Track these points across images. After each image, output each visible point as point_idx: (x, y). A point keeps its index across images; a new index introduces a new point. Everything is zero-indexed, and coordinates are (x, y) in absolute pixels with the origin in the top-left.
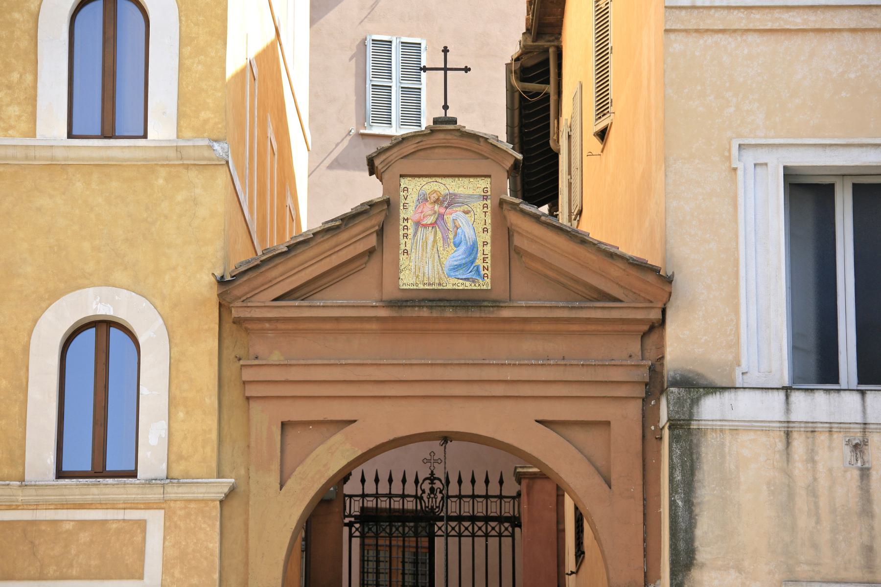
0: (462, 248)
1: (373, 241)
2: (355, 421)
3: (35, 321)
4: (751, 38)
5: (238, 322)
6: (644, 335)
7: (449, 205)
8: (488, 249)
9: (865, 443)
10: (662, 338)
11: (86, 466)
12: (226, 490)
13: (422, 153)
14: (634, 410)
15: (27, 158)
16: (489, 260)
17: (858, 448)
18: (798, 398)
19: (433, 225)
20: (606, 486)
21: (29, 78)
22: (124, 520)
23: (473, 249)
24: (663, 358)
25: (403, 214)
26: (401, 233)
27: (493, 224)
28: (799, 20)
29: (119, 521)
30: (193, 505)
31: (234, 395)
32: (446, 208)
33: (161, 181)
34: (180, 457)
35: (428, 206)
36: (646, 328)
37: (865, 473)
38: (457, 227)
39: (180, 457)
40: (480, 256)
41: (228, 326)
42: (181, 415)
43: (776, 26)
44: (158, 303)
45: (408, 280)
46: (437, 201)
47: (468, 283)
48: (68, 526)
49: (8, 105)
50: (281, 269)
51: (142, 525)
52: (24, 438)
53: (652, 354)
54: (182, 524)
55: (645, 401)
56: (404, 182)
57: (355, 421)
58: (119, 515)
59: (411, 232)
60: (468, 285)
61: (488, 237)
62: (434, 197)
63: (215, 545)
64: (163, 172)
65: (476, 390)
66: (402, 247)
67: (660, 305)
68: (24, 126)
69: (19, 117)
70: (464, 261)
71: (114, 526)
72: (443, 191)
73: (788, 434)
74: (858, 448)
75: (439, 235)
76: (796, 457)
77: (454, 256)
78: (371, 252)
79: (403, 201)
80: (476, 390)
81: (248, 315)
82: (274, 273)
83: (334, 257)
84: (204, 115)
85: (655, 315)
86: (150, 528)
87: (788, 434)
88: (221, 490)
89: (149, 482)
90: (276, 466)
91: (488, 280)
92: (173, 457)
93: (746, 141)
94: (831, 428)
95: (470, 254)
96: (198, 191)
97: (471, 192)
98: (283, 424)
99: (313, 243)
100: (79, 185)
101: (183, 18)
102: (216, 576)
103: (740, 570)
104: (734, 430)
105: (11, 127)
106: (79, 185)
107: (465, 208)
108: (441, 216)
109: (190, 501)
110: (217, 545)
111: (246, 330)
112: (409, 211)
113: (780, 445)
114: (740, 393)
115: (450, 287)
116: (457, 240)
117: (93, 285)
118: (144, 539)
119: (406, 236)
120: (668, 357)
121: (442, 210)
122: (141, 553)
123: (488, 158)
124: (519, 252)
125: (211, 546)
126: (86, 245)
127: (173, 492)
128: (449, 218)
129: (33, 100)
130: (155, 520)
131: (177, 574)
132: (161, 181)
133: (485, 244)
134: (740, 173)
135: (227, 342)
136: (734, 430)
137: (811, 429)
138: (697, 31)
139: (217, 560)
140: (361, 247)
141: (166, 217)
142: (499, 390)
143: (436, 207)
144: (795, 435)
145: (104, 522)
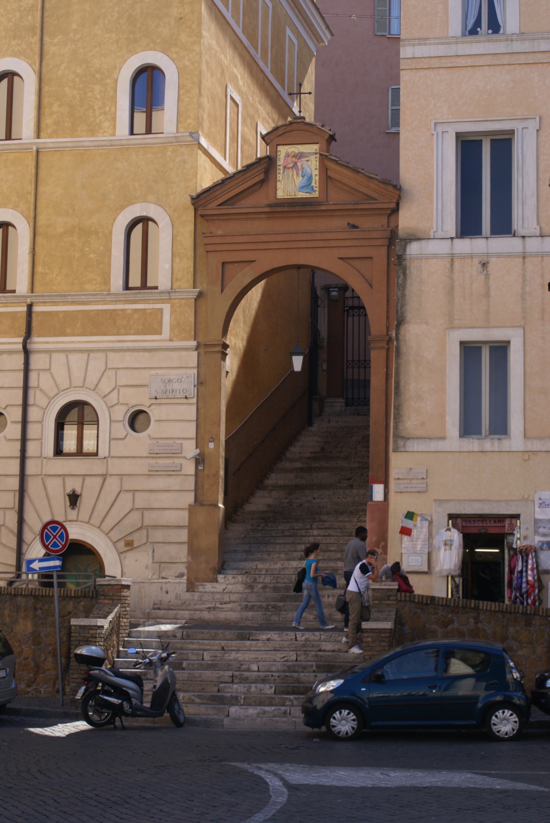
0: (306, 178)
1: (262, 177)
2: (255, 261)
3: (115, 220)
4: (442, 71)
5: (202, 216)
6: (389, 215)
7: (300, 158)
8: (317, 178)
9: (488, 262)
10: (398, 216)
11: (139, 285)
12: (197, 294)
13: (287, 134)
14: (384, 250)
15: (111, 146)
16: (318, 183)
17: (484, 265)
18: (457, 242)
19: (292, 168)
20: (369, 287)
21: (113, 109)
22: (153, 309)
23: (310, 178)
24: (398, 226)
25: (278, 163)
26: (278, 172)
27: (319, 166)
28: (463, 62)
29: (151, 309)
30: (183, 301)
31: (201, 250)
32: (298, 159)
33: (169, 153)
34: (177, 280)
35: (290, 158)
36: (389, 212)
37: (487, 276)
38: (303, 168)
39: (177, 280)
40: (314, 181)
41: (199, 218)
42: (177, 260)
43: (452, 65)
44: (167, 209)
45: (280, 194)
46: (294, 156)
47: (308, 194)
48: (129, 312)
49: (104, 122)
50: (220, 191)
51: (161, 311)
52: (110, 273)
53: (392, 225)
55: (389, 246)
56: (280, 148)
57: (255, 261)
59: (282, 171)
60: (308, 195)
61: (317, 172)
62: (293, 154)
63: (192, 319)
64: (170, 149)
65: (310, 244)
66: (278, 179)
67: (395, 201)
68: (110, 131)
69: (109, 127)
70: (306, 184)
71: (149, 311)
72: (297, 151)
73: (452, 260)
74: (484, 265)
75: (295, 172)
76: (455, 270)
77: (299, 181)
78: (262, 182)
79: (278, 157)
80: (310, 244)
81: (206, 213)
82: (217, 193)
83: (244, 184)
84: (189, 121)
85: (393, 205)
86: (164, 311)
87: (452, 260)
88: (194, 294)
89: (161, 292)
91: (317, 193)
92: (174, 280)
93: (438, 121)
94: (471, 256)
95: (309, 181)
97: (309, 151)
98: (223, 263)
99: (234, 179)
101: (180, 77)
102: (193, 333)
103: (427, 323)
104: (427, 258)
105: (105, 132)
107: (307, 159)
108: (296, 163)
110: (193, 319)
111: (207, 220)
112: (281, 161)
113: (448, 266)
114: (430, 241)
115: (299, 196)
116: (303, 174)
117: (139, 202)
119: (280, 173)
120: (400, 226)
121: (296, 161)
122: (161, 323)
123: (317, 135)
124: (331, 178)
125: (191, 319)
127: (173, 296)
128: (299, 164)
129: (114, 119)
130: (166, 308)
131: (176, 332)
132: (169, 153)
133: (316, 175)
134: (435, 136)
135: (199, 226)
136: (427, 258)
137: (463, 257)
138: (416, 69)
139: (193, 326)
140: (257, 179)
142: (321, 244)
143: (294, 159)
144: (456, 260)
145: (144, 310)
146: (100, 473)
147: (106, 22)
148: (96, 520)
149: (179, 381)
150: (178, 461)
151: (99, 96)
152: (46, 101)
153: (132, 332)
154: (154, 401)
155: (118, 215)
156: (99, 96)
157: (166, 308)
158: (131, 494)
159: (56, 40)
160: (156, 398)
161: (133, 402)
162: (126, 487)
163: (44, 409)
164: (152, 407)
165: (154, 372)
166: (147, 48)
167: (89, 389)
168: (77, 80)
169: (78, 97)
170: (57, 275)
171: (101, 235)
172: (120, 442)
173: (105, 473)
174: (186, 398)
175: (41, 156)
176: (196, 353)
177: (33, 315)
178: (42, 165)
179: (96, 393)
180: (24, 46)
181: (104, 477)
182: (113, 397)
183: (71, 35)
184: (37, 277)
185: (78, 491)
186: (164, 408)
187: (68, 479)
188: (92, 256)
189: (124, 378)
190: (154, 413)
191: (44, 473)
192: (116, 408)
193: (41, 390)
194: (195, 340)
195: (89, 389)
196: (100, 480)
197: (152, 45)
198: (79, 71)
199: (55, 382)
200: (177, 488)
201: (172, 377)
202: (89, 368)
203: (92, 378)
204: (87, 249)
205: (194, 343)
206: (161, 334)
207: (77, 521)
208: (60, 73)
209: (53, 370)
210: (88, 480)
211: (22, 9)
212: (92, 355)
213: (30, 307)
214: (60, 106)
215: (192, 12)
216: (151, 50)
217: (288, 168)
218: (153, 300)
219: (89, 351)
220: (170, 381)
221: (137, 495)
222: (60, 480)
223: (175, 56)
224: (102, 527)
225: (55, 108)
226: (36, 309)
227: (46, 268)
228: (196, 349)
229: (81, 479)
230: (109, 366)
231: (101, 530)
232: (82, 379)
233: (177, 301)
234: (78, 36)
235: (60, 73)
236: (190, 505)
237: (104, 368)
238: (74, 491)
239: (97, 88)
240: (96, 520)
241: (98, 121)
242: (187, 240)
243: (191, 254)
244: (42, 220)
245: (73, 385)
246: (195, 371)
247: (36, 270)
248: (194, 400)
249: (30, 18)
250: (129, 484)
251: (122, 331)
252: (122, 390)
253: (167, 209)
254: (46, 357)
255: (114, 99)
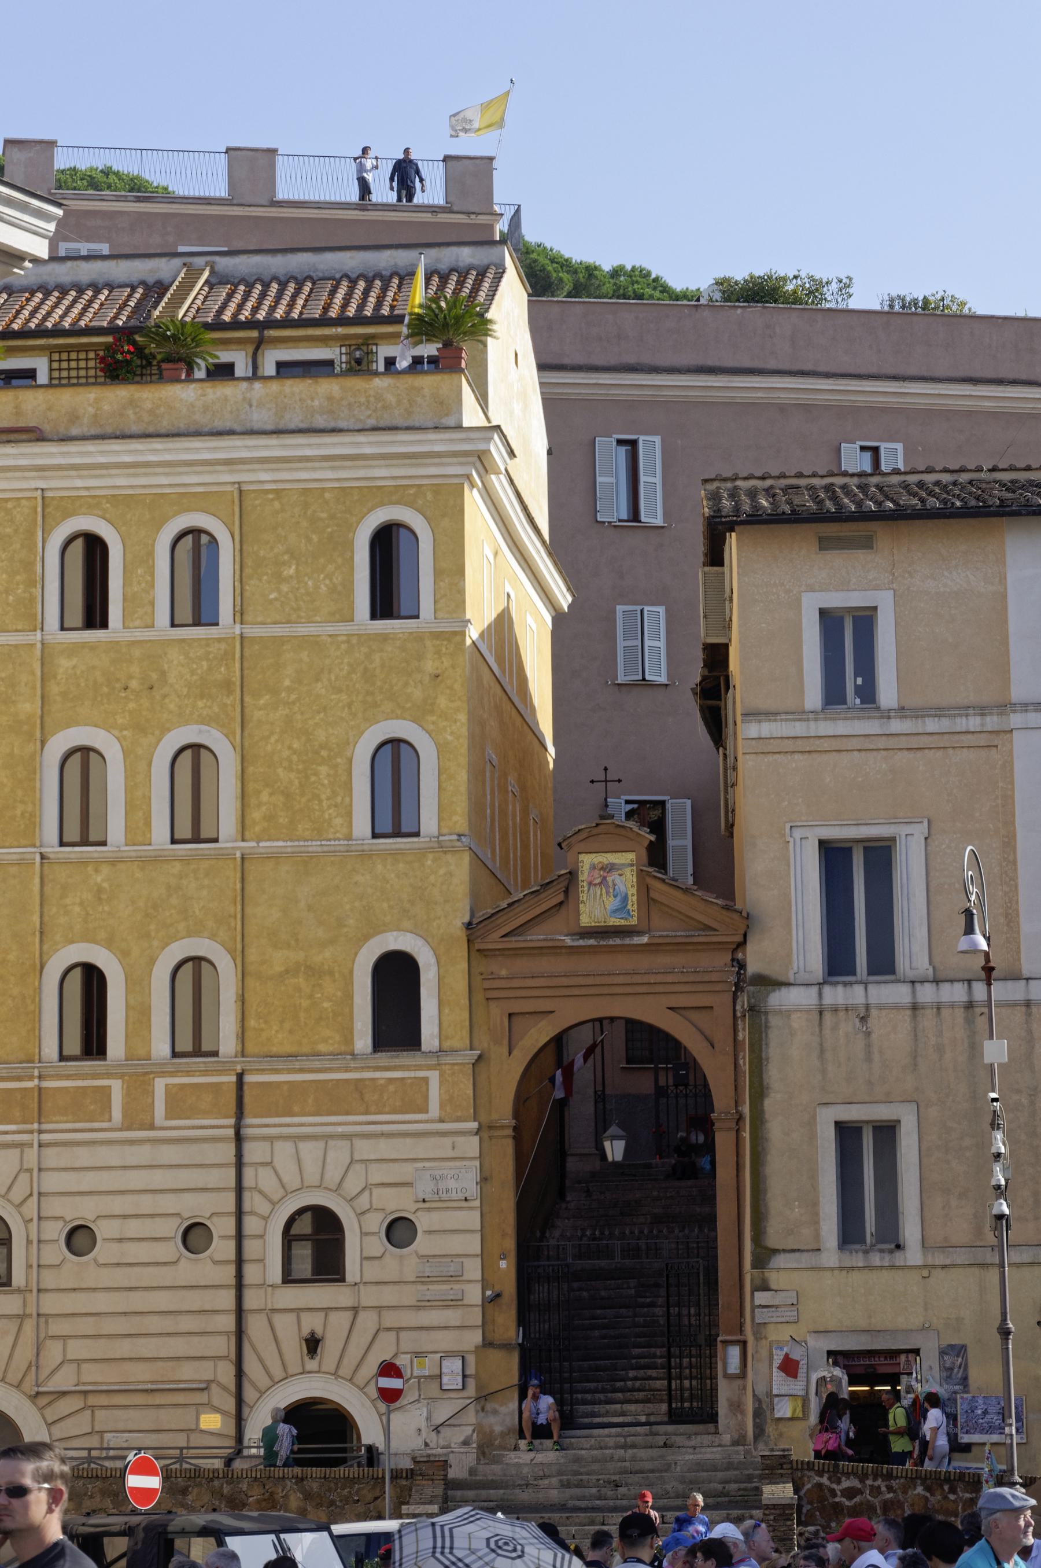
0: (619, 898)
3: (356, 954)
21: (347, 799)
31: (479, 997)
35: (597, 872)
38: (614, 885)
39: (447, 1038)
42: (447, 1011)
51: (426, 1080)
54: (450, 1079)
58: (412, 1074)
62: (600, 866)
63: (470, 1092)
75: (604, 891)
90: (506, 1042)
96: (452, 867)
100: (380, 867)
106: (380, 867)
109: (454, 1064)
117: (391, 931)
118: (428, 1090)
122: (426, 1098)
126: (385, 905)
130: (434, 1076)
141: (433, 885)
145: (403, 1079)
146: (350, 1304)
147: (333, 678)
148: (346, 1370)
149: (456, 1177)
150: (456, 1287)
151: (326, 782)
152: (251, 787)
153: (387, 1109)
154: (422, 1205)
155: (361, 947)
156: (326, 782)
157: (434, 1076)
158: (392, 1335)
159: (262, 702)
160: (424, 1201)
161: (391, 1206)
162: (387, 1324)
163: (266, 1219)
164: (419, 1214)
165: (420, 1165)
166: (392, 716)
167: (330, 1190)
168: (295, 758)
169: (296, 782)
170: (277, 1032)
171: (337, 975)
172: (376, 1262)
173: (356, 1305)
174: (466, 1199)
175: (247, 864)
176: (477, 1139)
177: (246, 1088)
178: (250, 878)
179: (339, 1195)
180: (216, 709)
181: (355, 1310)
182: (364, 1201)
183: (283, 695)
184: (249, 1034)
185: (319, 1332)
186: (435, 1216)
187: (304, 1316)
188: (326, 1005)
189: (378, 1175)
190: (423, 1222)
191: (270, 1307)
192: (368, 1215)
193: (261, 1192)
194: (475, 1120)
195: (330, 1190)
196: (349, 1315)
197: (399, 712)
198: (296, 745)
199: (280, 1180)
200: (458, 1324)
201: (445, 1172)
202: (328, 1160)
203: (333, 1175)
204: (319, 995)
205: (474, 1125)
206: (427, 1112)
207: (318, 1372)
208: (269, 748)
209: (277, 1163)
210: (333, 1316)
211: (211, 656)
212: (331, 1143)
213: (240, 1076)
214: (271, 794)
215: (453, 667)
216: (397, 718)
217: (595, 885)
218: (415, 1066)
219: (328, 1137)
220: (442, 1177)
221: (403, 1335)
222: (292, 1317)
223: (432, 727)
224: (355, 1380)
225: (265, 797)
226: (248, 1078)
227: (261, 1021)
228: (476, 1134)
229: (322, 1314)
230: (357, 1157)
231: (353, 1384)
232: (318, 1177)
233: (447, 1067)
234: (293, 697)
235: (269, 748)
236: (476, 1347)
237: (349, 1161)
238: (313, 1334)
239: (323, 770)
240: (346, 1370)
241: (327, 816)
242: (460, 984)
243: (465, 1001)
244: (252, 955)
245: (306, 1184)
246: (477, 1163)
247: (247, 1024)
248: (477, 1203)
249: (223, 669)
250: (390, 1319)
251: (373, 1109)
252: (376, 1191)
253: (430, 940)
254: (266, 1145)
255: (348, 786)
